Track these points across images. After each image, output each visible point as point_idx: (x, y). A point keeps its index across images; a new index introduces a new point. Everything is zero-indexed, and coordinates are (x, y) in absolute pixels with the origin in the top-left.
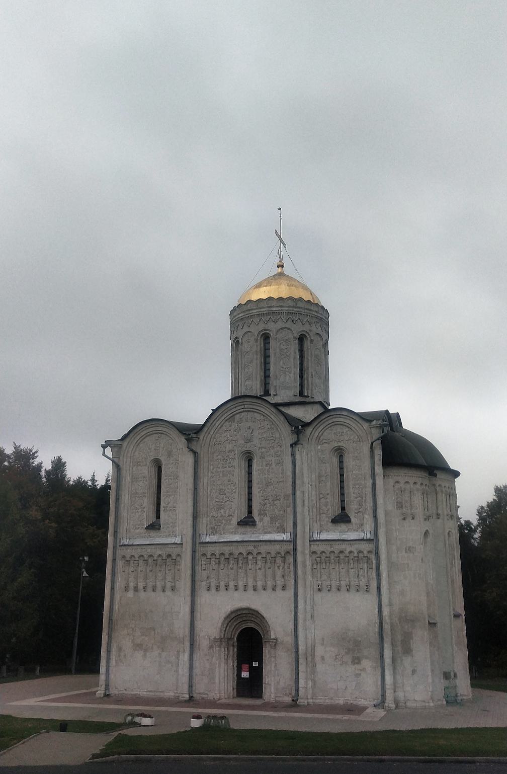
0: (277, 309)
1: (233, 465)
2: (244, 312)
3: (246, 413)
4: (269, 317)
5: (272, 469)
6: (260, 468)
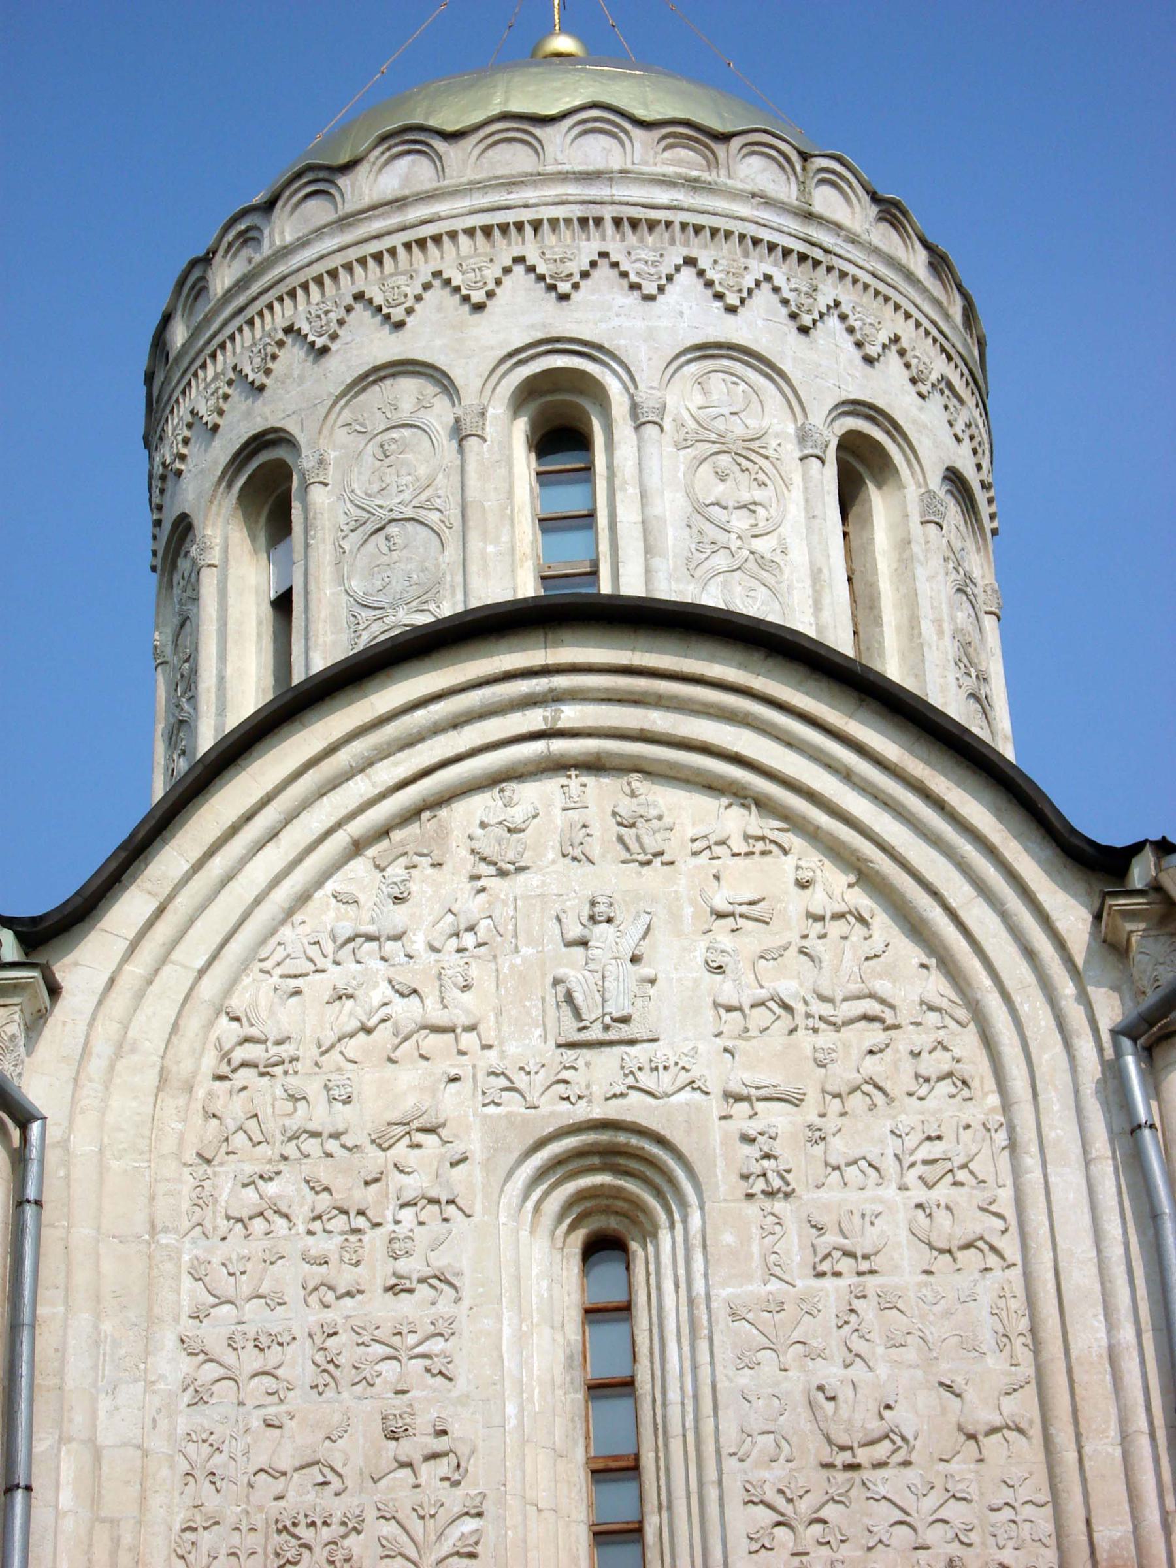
0: (662, 196)
1: (440, 1261)
2: (344, 222)
3: (549, 788)
4: (588, 248)
5: (888, 1304)
6: (757, 1288)
